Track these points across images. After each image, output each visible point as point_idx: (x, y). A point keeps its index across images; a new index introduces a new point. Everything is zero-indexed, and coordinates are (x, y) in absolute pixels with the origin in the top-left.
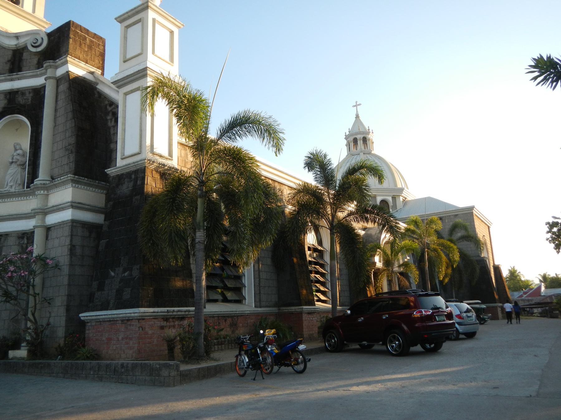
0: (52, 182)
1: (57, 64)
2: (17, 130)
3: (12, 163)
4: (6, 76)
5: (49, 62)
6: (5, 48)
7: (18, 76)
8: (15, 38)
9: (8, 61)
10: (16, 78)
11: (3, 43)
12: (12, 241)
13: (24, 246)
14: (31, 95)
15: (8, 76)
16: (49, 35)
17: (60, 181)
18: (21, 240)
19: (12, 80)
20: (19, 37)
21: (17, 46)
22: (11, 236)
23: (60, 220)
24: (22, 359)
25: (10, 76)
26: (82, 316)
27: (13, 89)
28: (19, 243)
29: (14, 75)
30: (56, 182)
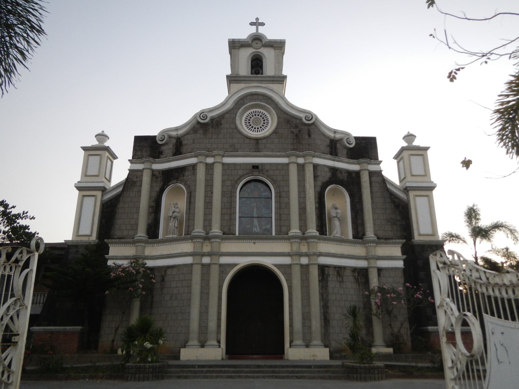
0: (386, 241)
1: (371, 162)
2: (333, 195)
3: (336, 217)
4: (329, 156)
5: (368, 160)
6: (324, 135)
7: (339, 159)
8: (334, 132)
9: (328, 146)
10: (336, 160)
11: (325, 132)
12: (348, 273)
13: (357, 277)
14: (346, 174)
15: (333, 157)
16: (356, 138)
17: (394, 242)
18: (354, 273)
19: (334, 160)
20: (336, 133)
21: (335, 138)
22: (347, 269)
23: (390, 266)
24: (390, 353)
25: (334, 157)
26: (430, 329)
27: (335, 167)
28: (353, 275)
29: (337, 158)
30: (389, 242)
